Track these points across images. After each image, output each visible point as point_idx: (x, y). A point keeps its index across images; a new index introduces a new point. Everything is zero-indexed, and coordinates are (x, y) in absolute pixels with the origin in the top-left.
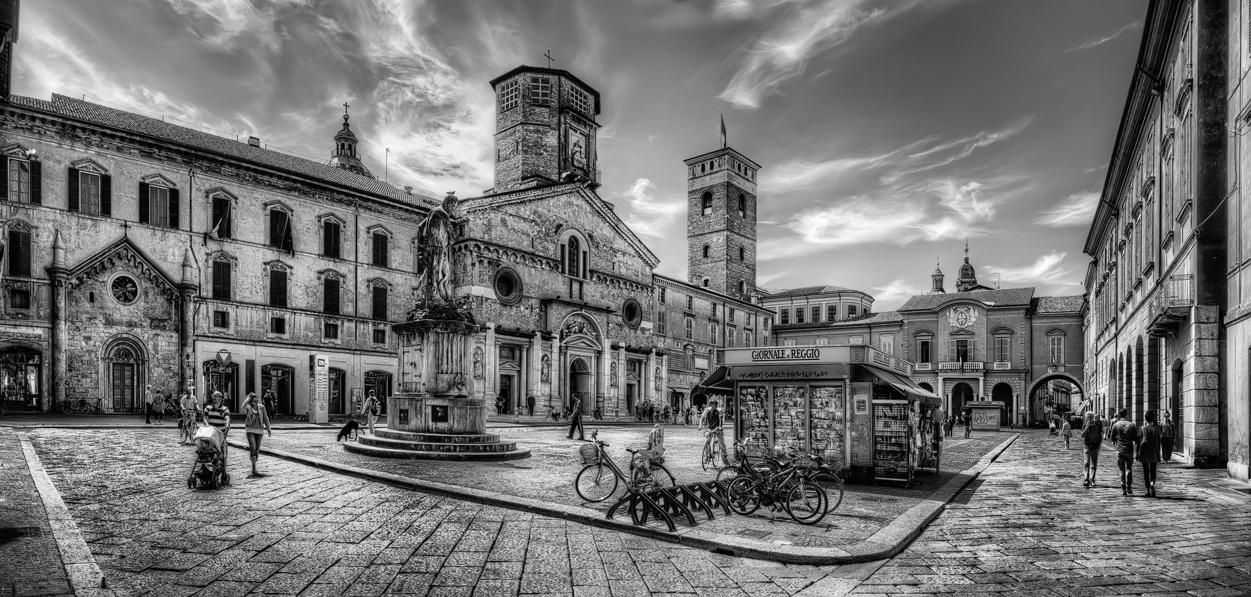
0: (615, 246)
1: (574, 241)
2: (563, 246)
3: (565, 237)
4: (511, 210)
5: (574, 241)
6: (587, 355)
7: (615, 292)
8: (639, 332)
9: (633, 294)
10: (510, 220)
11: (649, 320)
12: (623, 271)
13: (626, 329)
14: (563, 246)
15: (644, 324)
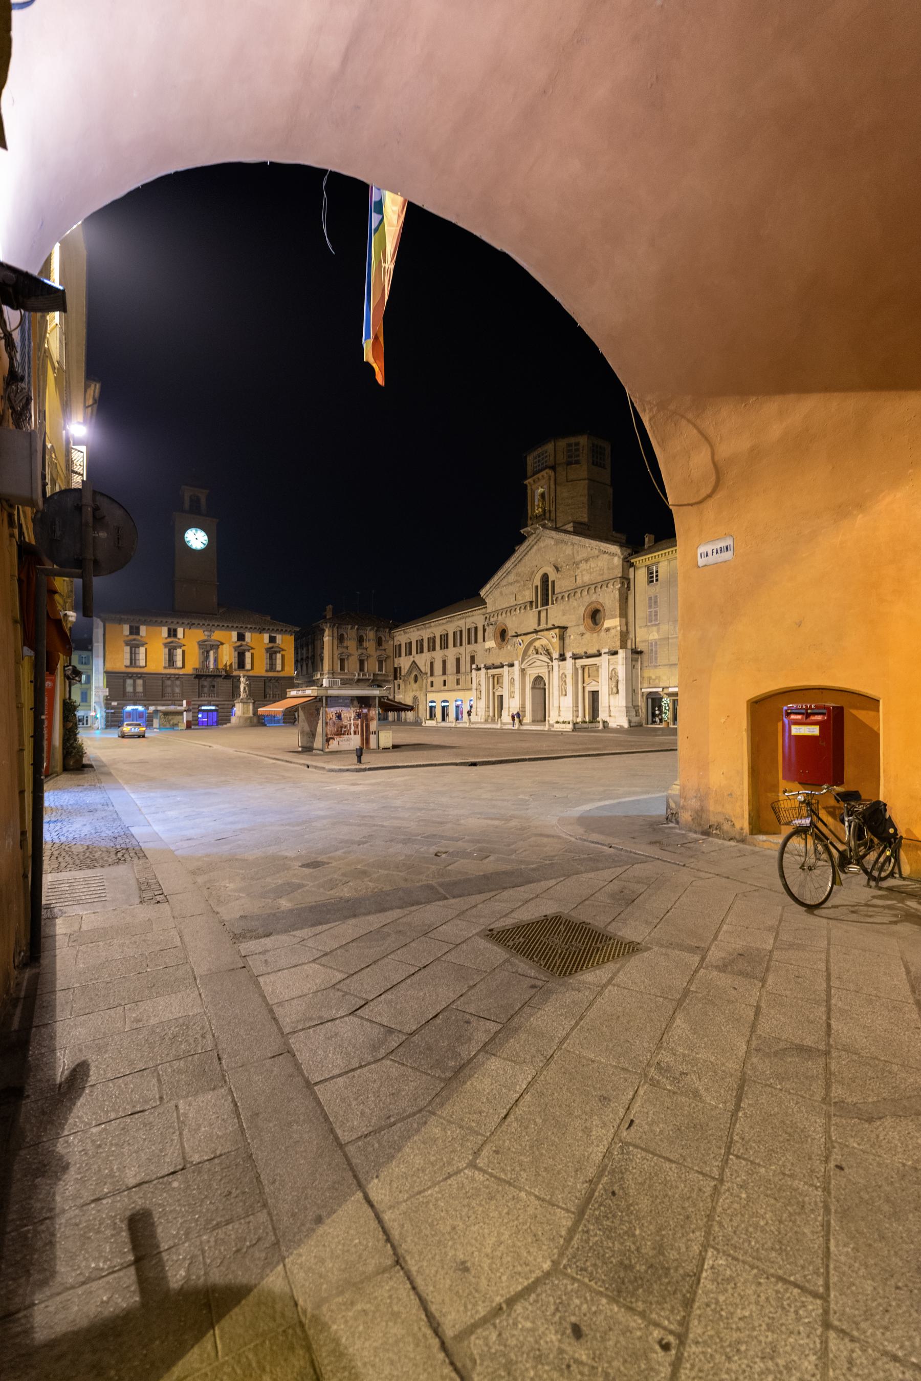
0: (578, 558)
1: (545, 578)
2: (537, 587)
3: (537, 581)
4: (504, 583)
5: (545, 578)
6: (543, 672)
7: (575, 603)
8: (603, 633)
9: (594, 598)
10: (505, 590)
11: (613, 617)
12: (587, 578)
13: (588, 635)
14: (537, 587)
15: (608, 623)
